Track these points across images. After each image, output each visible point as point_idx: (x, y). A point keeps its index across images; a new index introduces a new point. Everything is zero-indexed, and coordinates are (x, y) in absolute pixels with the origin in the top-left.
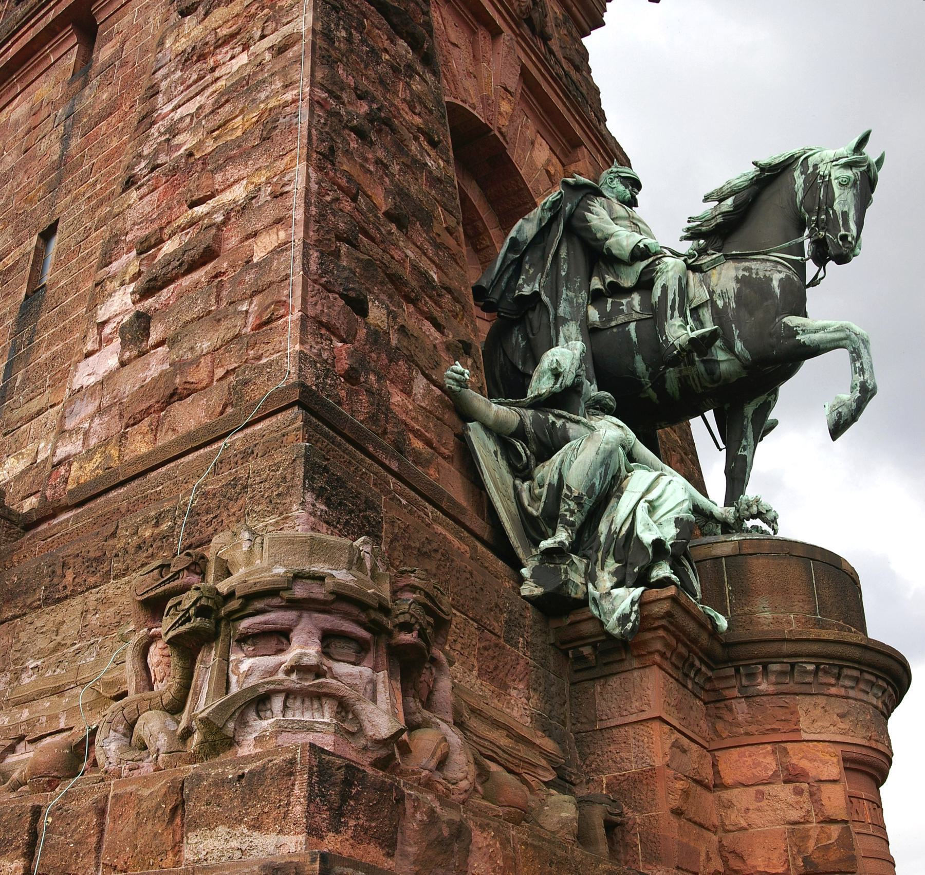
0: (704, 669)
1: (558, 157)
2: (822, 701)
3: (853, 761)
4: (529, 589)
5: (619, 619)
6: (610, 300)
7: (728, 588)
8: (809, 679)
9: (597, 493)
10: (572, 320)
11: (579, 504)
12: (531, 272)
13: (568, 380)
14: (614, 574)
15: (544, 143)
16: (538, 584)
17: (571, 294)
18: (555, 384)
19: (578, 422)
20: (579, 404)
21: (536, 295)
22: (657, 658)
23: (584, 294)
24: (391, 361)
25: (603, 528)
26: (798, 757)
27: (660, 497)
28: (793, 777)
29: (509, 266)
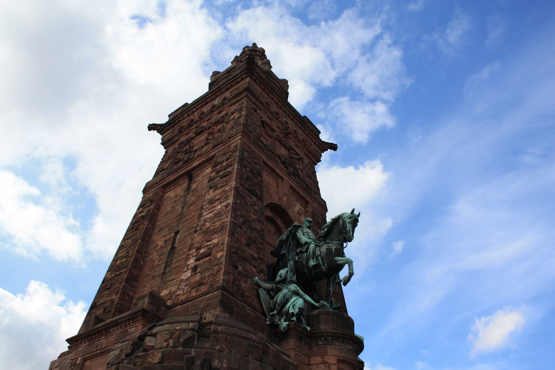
0: (306, 339)
1: (303, 207)
2: (333, 346)
3: (341, 360)
4: (268, 323)
5: (283, 328)
6: (300, 254)
7: (315, 322)
8: (331, 341)
11: (279, 305)
13: (283, 277)
14: (284, 319)
15: (299, 204)
16: (269, 321)
17: (292, 253)
19: (285, 287)
21: (285, 253)
22: (293, 336)
23: (295, 253)
24: (242, 278)
25: (284, 310)
26: (326, 358)
27: (296, 303)
28: (325, 363)
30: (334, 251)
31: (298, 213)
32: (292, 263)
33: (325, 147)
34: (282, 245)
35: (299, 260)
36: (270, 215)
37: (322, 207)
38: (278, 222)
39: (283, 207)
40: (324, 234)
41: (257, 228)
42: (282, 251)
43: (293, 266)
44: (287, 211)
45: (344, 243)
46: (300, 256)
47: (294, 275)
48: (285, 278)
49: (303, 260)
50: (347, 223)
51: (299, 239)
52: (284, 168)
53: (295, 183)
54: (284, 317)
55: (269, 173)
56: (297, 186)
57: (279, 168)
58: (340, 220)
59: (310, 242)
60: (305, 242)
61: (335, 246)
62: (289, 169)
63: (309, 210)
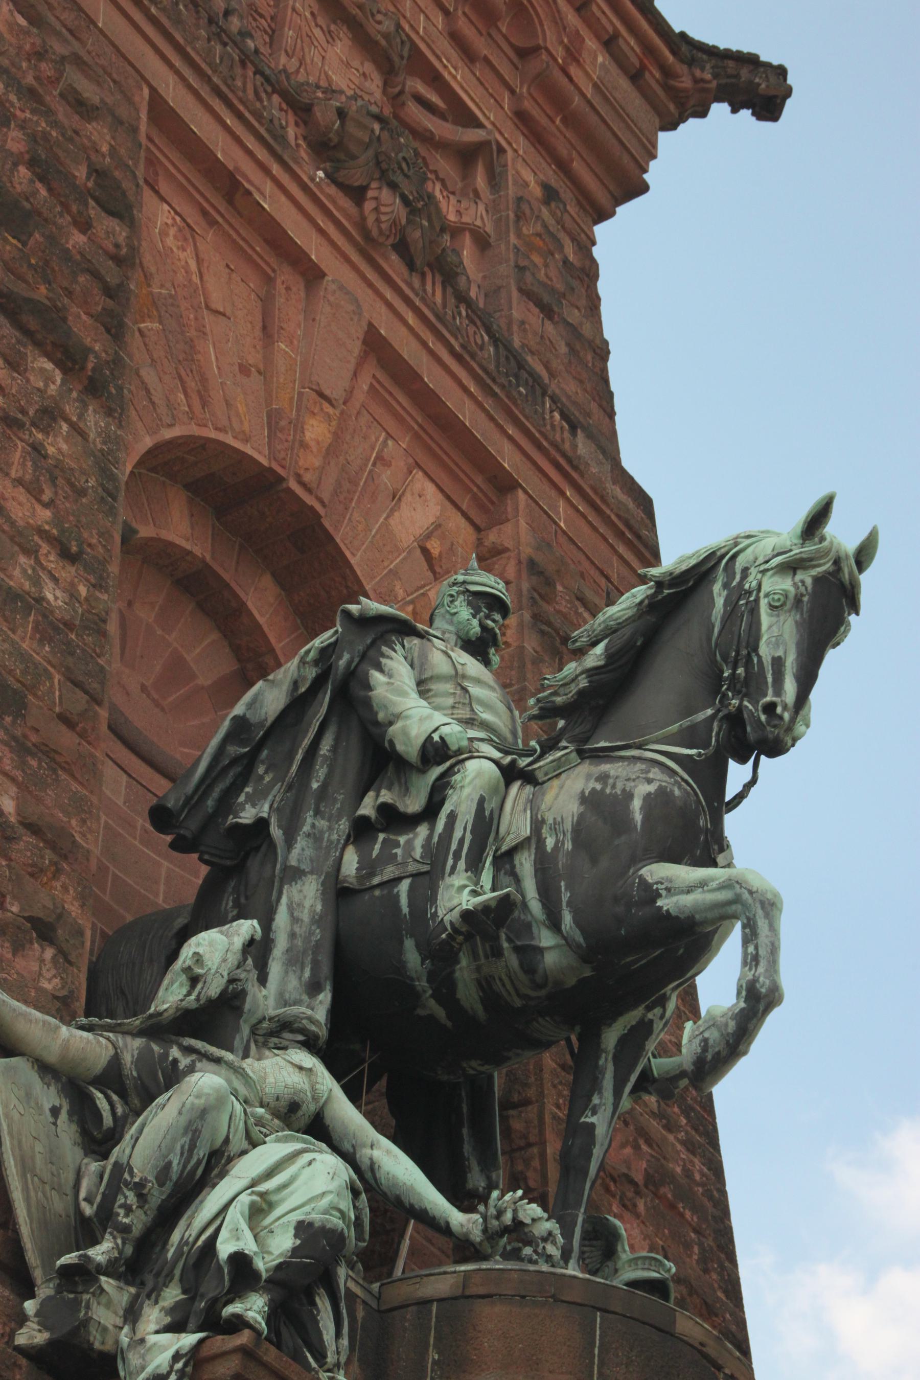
1: (465, 515)
6: (381, 836)
9: (174, 1177)
10: (312, 873)
11: (142, 1197)
12: (267, 779)
13: (214, 989)
14: (171, 1311)
15: (430, 488)
16: (44, 1325)
17: (322, 824)
18: (189, 994)
20: (237, 1029)
21: (261, 824)
23: (344, 825)
25: (175, 1237)
29: (226, 769)
30: (638, 817)
31: (418, 551)
32: (307, 903)
33: (686, 82)
34: (249, 762)
35: (372, 874)
36: (188, 547)
37: (620, 535)
38: (250, 604)
39: (293, 485)
40: (581, 693)
41: (50, 597)
42: (244, 809)
43: (318, 921)
44: (327, 524)
45: (731, 762)
46: (377, 847)
47: (314, 988)
48: (223, 993)
49: (398, 880)
50: (763, 603)
51: (381, 716)
52: (332, 190)
53: (411, 319)
54: (172, 1294)
55: (205, 213)
56: (424, 344)
57: (285, 179)
58: (714, 581)
59: (465, 743)
60: (430, 738)
61: (649, 781)
62: (369, 206)
63: (508, 544)
